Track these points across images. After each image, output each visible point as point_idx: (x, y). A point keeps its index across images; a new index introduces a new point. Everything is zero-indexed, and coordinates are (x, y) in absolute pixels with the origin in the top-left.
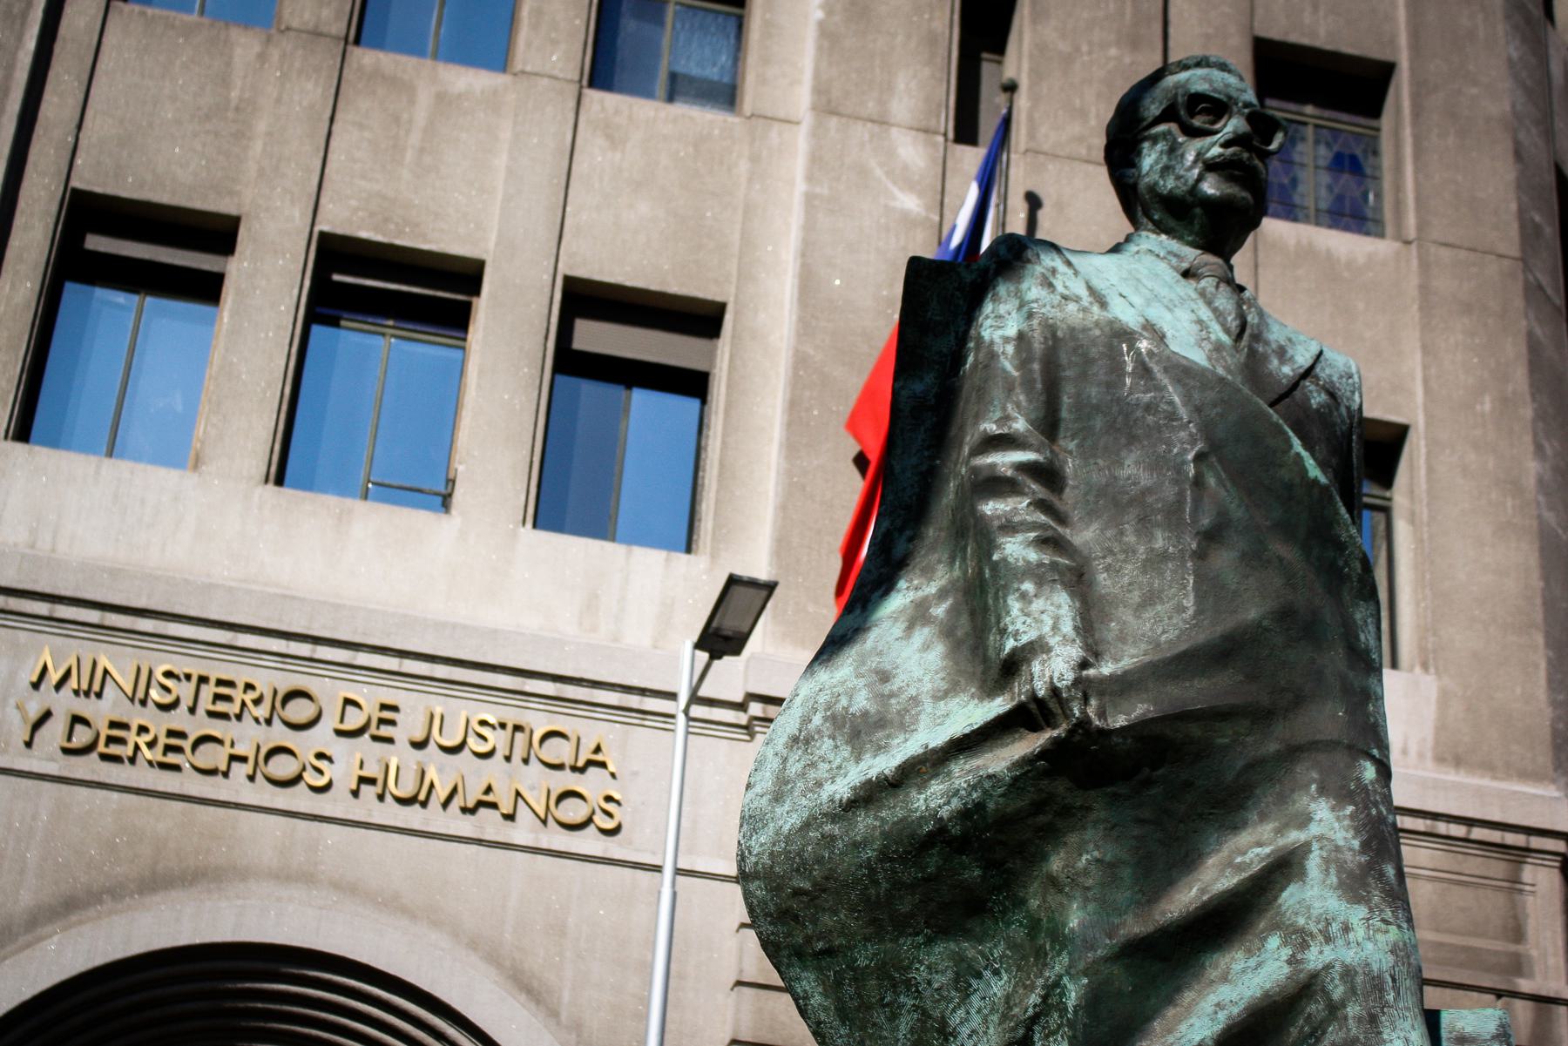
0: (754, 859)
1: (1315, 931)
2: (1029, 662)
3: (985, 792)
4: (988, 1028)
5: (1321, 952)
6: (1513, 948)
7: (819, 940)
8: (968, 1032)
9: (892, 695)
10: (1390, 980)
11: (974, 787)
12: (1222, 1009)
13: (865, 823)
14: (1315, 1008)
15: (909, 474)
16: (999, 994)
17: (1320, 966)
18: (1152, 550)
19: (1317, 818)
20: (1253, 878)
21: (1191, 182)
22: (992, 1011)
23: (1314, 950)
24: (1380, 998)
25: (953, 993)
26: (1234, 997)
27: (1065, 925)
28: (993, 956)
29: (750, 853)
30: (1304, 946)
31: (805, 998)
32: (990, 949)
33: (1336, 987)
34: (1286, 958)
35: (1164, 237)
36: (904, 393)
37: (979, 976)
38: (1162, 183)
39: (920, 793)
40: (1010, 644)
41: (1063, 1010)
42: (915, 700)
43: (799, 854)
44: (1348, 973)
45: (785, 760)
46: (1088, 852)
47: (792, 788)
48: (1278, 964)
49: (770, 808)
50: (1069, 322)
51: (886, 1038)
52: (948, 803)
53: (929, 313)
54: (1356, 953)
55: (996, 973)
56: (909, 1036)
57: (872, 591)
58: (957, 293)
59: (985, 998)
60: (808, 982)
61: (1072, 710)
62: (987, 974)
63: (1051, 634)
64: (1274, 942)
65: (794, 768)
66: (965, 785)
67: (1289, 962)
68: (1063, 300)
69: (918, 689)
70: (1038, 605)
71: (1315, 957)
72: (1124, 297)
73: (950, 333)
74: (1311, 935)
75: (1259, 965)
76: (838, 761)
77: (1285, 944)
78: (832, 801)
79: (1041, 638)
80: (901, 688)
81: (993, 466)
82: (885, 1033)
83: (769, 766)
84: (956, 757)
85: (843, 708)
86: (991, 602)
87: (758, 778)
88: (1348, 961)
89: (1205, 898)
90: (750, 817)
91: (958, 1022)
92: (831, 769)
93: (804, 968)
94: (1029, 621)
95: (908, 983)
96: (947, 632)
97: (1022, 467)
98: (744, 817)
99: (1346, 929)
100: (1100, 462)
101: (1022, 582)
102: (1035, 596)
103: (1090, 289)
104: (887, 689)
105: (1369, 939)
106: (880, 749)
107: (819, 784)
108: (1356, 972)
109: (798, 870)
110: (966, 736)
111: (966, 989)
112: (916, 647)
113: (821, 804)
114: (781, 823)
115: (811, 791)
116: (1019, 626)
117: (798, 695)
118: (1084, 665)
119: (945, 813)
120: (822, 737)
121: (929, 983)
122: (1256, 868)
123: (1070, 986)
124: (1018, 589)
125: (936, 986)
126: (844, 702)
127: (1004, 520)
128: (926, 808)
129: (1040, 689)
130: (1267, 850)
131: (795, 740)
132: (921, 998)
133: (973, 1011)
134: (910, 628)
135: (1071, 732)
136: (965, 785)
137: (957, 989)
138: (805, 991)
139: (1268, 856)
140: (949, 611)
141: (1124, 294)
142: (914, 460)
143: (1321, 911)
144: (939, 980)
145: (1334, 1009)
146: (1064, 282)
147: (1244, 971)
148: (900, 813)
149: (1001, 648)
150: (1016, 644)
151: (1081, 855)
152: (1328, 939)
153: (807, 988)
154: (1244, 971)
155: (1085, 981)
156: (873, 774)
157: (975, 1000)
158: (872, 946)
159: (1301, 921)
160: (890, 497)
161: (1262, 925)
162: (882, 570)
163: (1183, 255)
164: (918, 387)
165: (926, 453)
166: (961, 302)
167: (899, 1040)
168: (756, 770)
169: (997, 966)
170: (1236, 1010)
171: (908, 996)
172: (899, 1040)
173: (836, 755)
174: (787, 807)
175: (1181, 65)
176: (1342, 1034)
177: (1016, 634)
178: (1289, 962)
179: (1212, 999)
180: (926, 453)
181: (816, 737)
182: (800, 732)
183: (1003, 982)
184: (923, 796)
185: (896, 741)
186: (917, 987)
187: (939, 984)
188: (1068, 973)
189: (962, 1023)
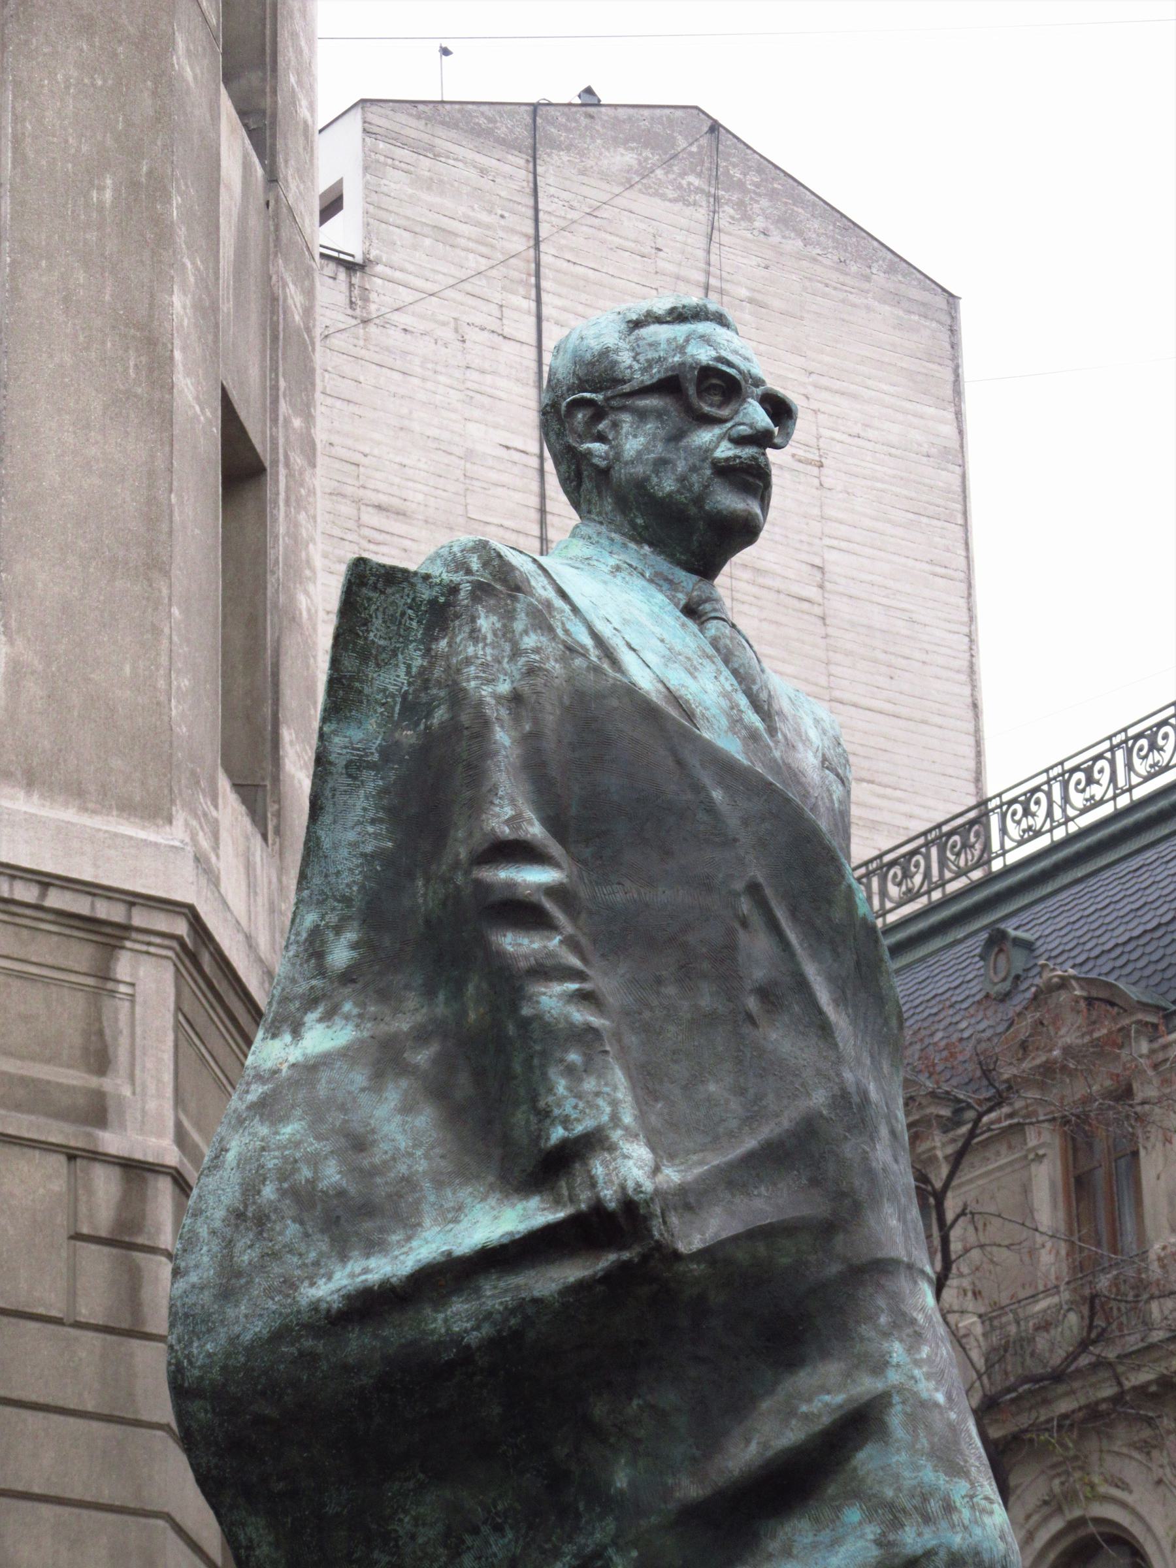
0: (197, 1373)
1: (908, 1506)
5: (920, 1535)
6: (94, 1082)
9: (374, 1171)
11: (512, 1312)
15: (344, 852)
16: (500, 1555)
17: (920, 1552)
19: (894, 1361)
21: (696, 487)
25: (441, 1550)
28: (495, 1508)
29: (190, 1363)
30: (896, 1524)
34: (871, 1537)
35: (646, 549)
36: (336, 740)
37: (475, 1531)
38: (655, 480)
39: (437, 1311)
40: (558, 1134)
42: (409, 1182)
45: (229, 1244)
46: (639, 1396)
47: (248, 1283)
48: (860, 1543)
49: (216, 1307)
50: (577, 684)
52: (477, 1328)
53: (372, 634)
54: (963, 1539)
55: (498, 1529)
58: (410, 612)
59: (480, 1558)
61: (649, 1231)
62: (485, 1529)
63: (611, 1125)
64: (853, 1515)
66: (501, 1308)
67: (879, 1543)
69: (410, 1167)
71: (913, 1539)
72: (634, 650)
73: (397, 665)
74: (904, 1510)
75: (835, 1542)
76: (313, 1255)
77: (869, 1517)
80: (385, 1162)
81: (511, 885)
83: (205, 1248)
85: (307, 1181)
86: (518, 1068)
87: (192, 1263)
88: (955, 1547)
90: (186, 1315)
94: (581, 1105)
97: (552, 891)
98: (176, 1313)
99: (949, 1508)
100: (628, 884)
101: (566, 1051)
102: (585, 1071)
105: (976, 1522)
106: (373, 1246)
107: (290, 1284)
109: (263, 1393)
112: (392, 1104)
114: (237, 1329)
116: (568, 1109)
117: (227, 1151)
118: (656, 1170)
119: (473, 1338)
120: (283, 1218)
121: (413, 1537)
122: (826, 1420)
124: (562, 1061)
125: (420, 1541)
126: (306, 1173)
127: (532, 959)
128: (447, 1330)
129: (611, 1201)
130: (839, 1398)
131: (238, 1216)
135: (645, 1258)
136: (501, 1308)
137: (445, 1546)
138: (251, 1540)
139: (841, 1406)
140: (435, 1061)
142: (351, 836)
143: (914, 1482)
144: (426, 1534)
146: (563, 624)
147: (815, 1546)
148: (409, 1334)
149: (539, 1136)
150: (566, 1134)
151: (631, 1399)
152: (927, 1519)
153: (254, 1536)
155: (635, 1554)
156: (373, 1278)
159: (889, 1493)
160: (317, 880)
161: (831, 1490)
162: (314, 982)
163: (676, 581)
166: (414, 624)
168: (185, 1251)
169: (499, 1521)
173: (309, 1246)
174: (243, 1309)
175: (675, 315)
177: (566, 1122)
178: (879, 1543)
180: (371, 829)
181: (273, 1217)
182: (246, 1206)
183: (506, 1540)
184: (441, 1316)
185: (394, 1238)
186: (396, 1541)
187: (425, 1539)
188: (614, 1543)
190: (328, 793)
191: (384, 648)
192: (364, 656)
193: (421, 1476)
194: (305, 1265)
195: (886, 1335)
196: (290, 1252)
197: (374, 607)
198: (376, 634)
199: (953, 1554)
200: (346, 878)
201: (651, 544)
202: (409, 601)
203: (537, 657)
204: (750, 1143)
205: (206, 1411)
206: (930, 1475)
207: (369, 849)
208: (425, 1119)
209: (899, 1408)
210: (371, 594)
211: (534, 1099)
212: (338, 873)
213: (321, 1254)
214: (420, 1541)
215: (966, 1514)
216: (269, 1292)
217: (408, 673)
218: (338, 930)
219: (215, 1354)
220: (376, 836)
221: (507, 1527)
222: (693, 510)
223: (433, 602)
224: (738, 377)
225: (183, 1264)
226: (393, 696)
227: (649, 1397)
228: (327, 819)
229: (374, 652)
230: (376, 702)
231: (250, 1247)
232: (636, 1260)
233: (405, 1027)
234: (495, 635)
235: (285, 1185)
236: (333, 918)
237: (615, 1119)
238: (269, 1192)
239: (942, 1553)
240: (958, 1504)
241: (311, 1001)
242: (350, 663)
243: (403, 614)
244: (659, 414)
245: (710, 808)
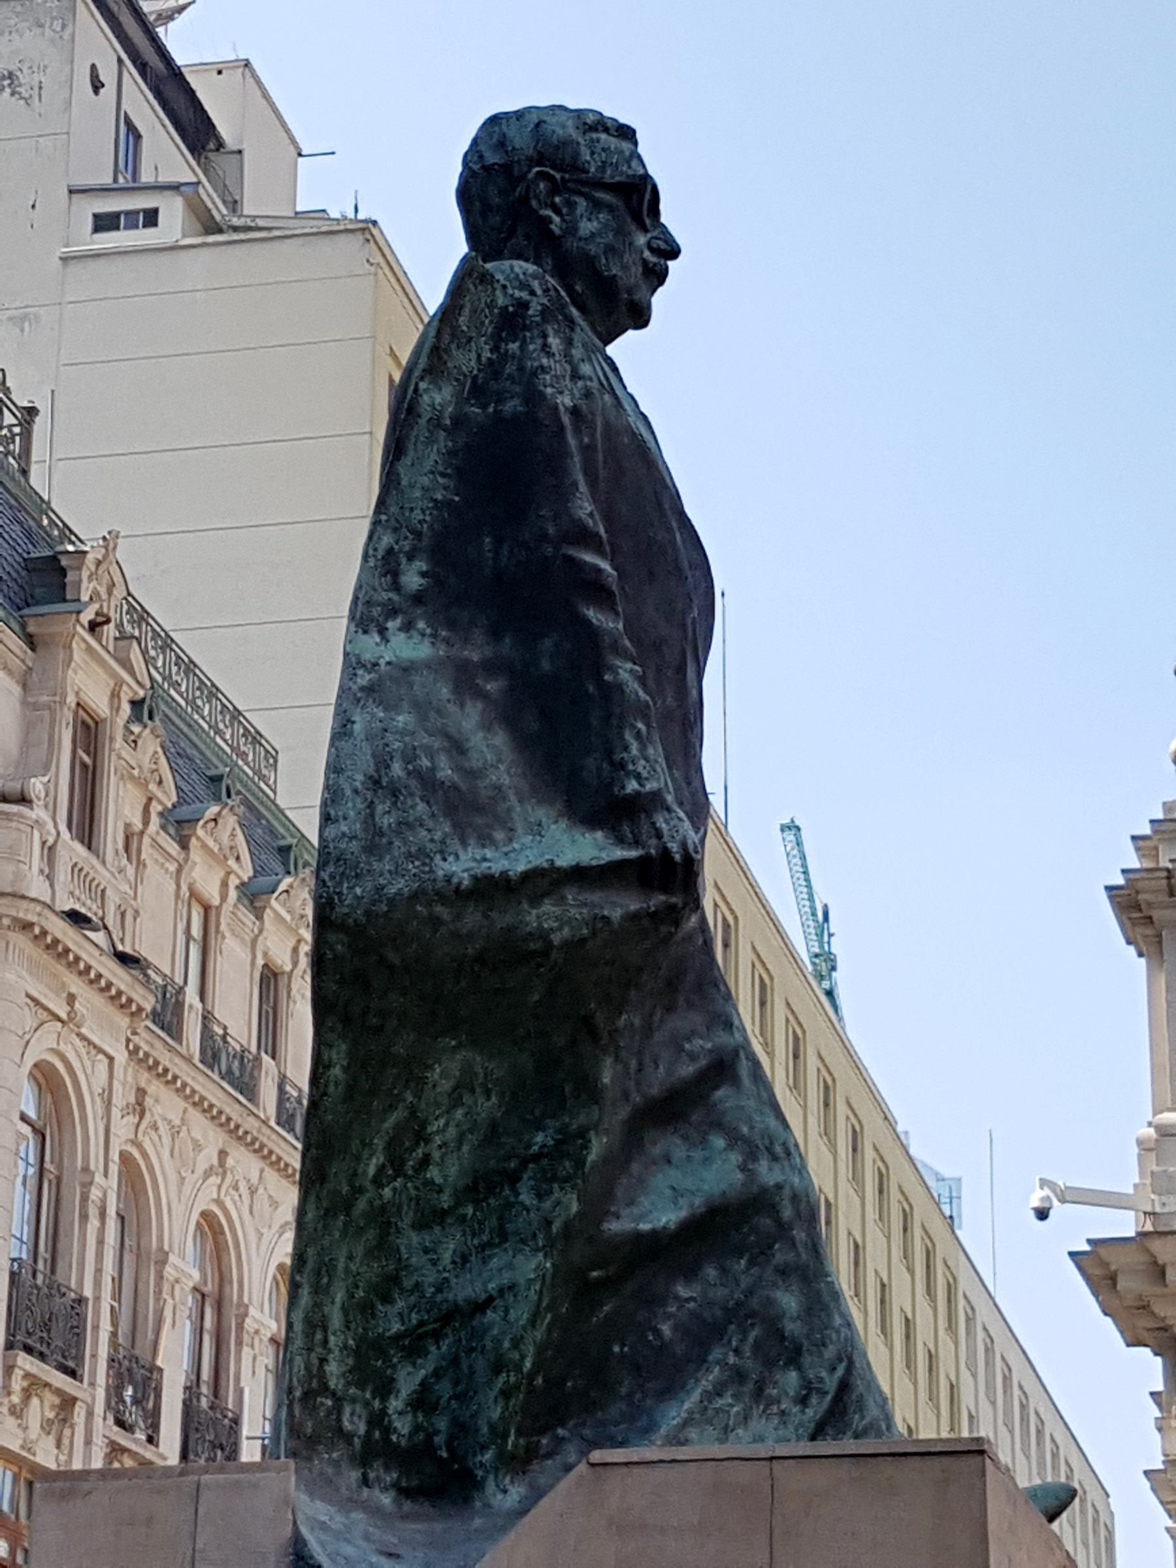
0: (346, 910)
13: (472, 918)
15: (418, 494)
22: (471, 1131)
37: (473, 1091)
39: (534, 908)
40: (632, 786)
41: (580, 1163)
55: (488, 1094)
60: (338, 1054)
95: (422, 1081)
115: (418, 859)
116: (640, 769)
119: (556, 939)
123: (594, 1142)
131: (375, 782)
142: (425, 480)
144: (446, 1086)
148: (508, 919)
151: (621, 1013)
157: (459, 1113)
160: (393, 509)
177: (638, 777)
183: (490, 1103)
184: (534, 912)
189: (438, 1131)
194: (432, 840)
196: (421, 825)
200: (417, 515)
208: (500, 739)
211: (609, 753)
212: (412, 510)
213: (446, 835)
216: (410, 856)
218: (411, 558)
219: (363, 897)
220: (446, 488)
221: (494, 1093)
225: (332, 813)
228: (407, 460)
233: (476, 657)
235: (410, 767)
236: (406, 545)
238: (397, 769)
241: (392, 612)
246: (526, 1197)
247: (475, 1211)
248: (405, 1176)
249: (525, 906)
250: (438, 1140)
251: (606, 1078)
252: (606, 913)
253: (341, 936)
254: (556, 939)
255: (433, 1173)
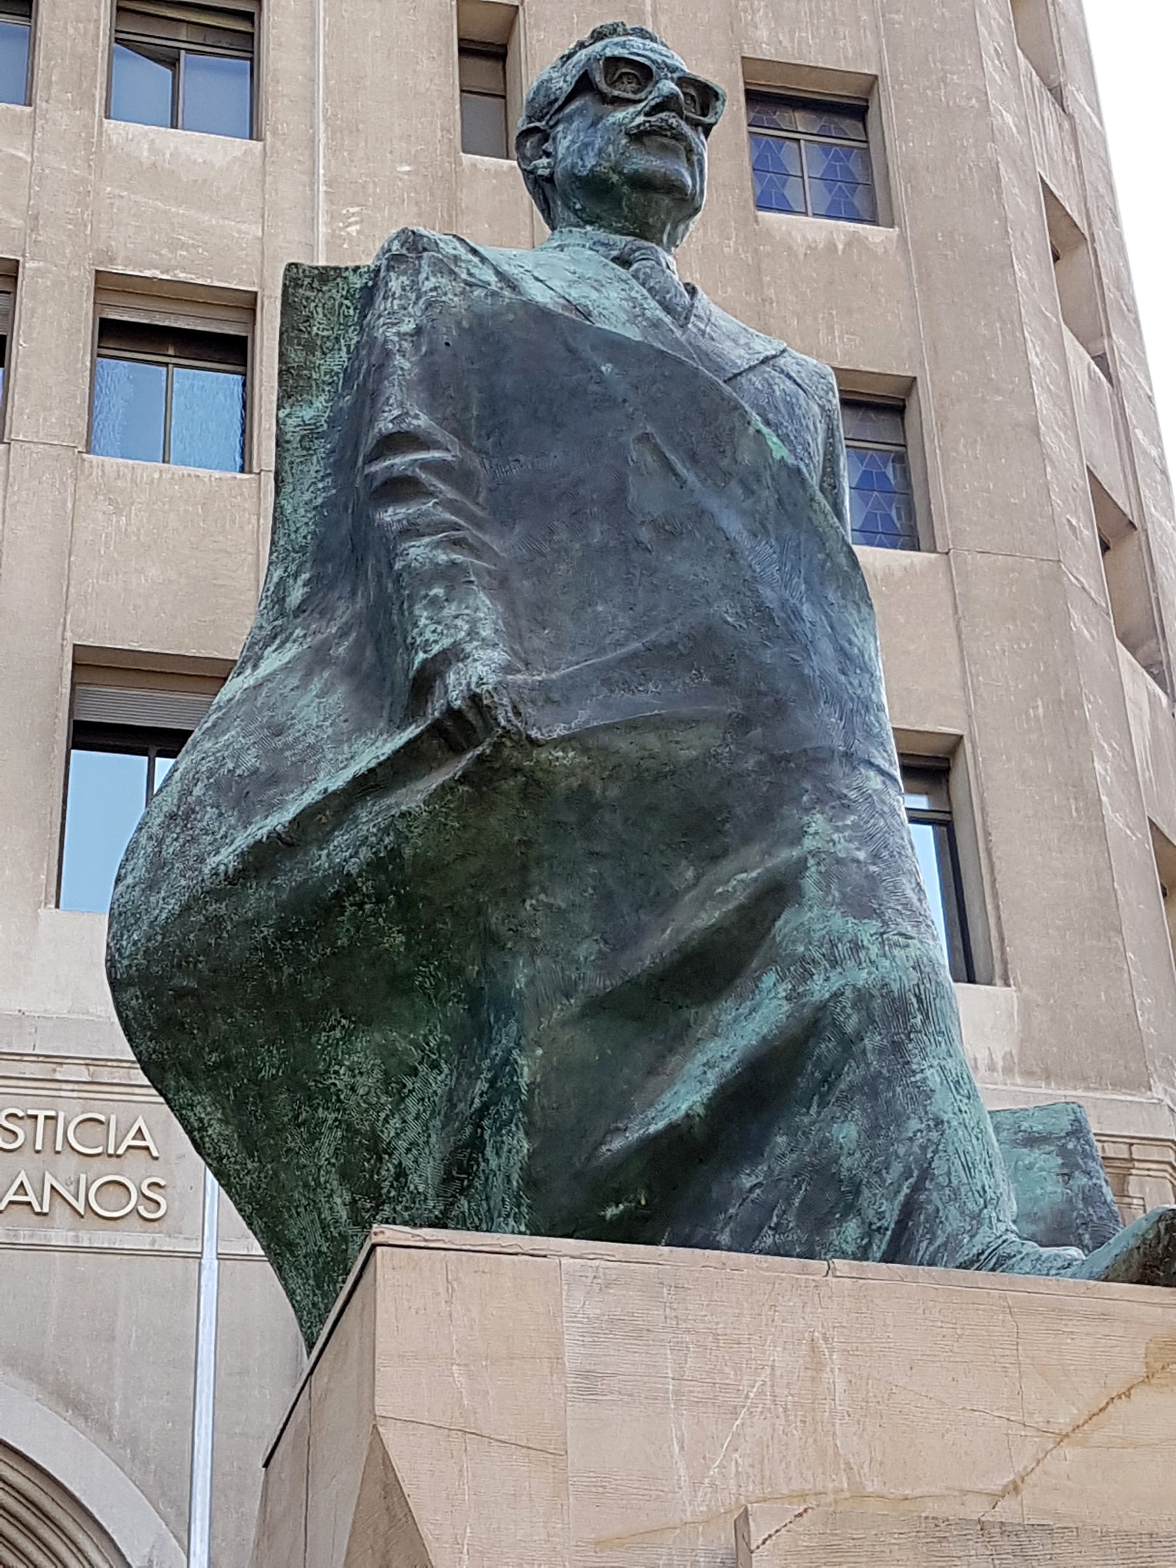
0: (126, 962)
1: (817, 956)
2: (441, 675)
3: (398, 833)
4: (429, 1136)
5: (827, 979)
7: (210, 1053)
8: (406, 1145)
10: (914, 1000)
11: (386, 831)
12: (713, 1067)
13: (256, 897)
14: (826, 1048)
16: (439, 1092)
17: (827, 995)
18: (588, 545)
20: (741, 908)
22: (433, 1116)
23: (818, 979)
24: (905, 1023)
25: (384, 1099)
26: (725, 1051)
27: (510, 987)
28: (428, 1044)
31: (200, 1130)
32: (425, 1036)
33: (849, 1016)
34: (784, 994)
37: (414, 1072)
39: (322, 849)
40: (421, 656)
43: (179, 946)
44: (862, 998)
45: (160, 842)
46: (532, 898)
48: (776, 1002)
50: (475, 310)
51: (305, 1166)
53: (315, 329)
54: (869, 973)
55: (435, 1066)
56: (333, 1161)
57: (266, 646)
58: (347, 302)
59: (423, 1099)
60: (205, 1108)
62: (423, 1069)
64: (769, 979)
65: (169, 850)
66: (375, 830)
67: (788, 998)
68: (468, 288)
70: (450, 610)
71: (819, 988)
72: (541, 281)
73: (340, 349)
75: (754, 1010)
78: (217, 874)
79: (455, 644)
82: (303, 1161)
84: (362, 798)
85: (229, 771)
86: (395, 618)
89: (682, 938)
91: (392, 1134)
92: (216, 840)
93: (197, 1091)
94: (440, 628)
96: (351, 670)
99: (857, 946)
102: (447, 600)
103: (498, 273)
104: (279, 743)
105: (885, 955)
106: (271, 808)
107: (201, 860)
108: (872, 996)
109: (180, 965)
110: (371, 771)
111: (399, 1092)
113: (203, 880)
116: (428, 635)
119: (353, 867)
121: (353, 1089)
122: (741, 897)
124: (427, 596)
125: (361, 1091)
127: (405, 522)
130: (754, 874)
132: (345, 1110)
133: (410, 1118)
134: (308, 676)
135: (498, 746)
136: (375, 830)
138: (201, 1120)
141: (541, 278)
142: (307, 496)
143: (824, 932)
144: (365, 1084)
145: (849, 1044)
147: (736, 1020)
148: (299, 877)
150: (425, 656)
151: (524, 901)
152: (834, 964)
153: (203, 1115)
154: (736, 1020)
155: (540, 1052)
157: (412, 1105)
158: (278, 1049)
164: (308, 414)
165: (320, 485)
166: (351, 312)
167: (321, 1167)
169: (434, 1057)
170: (728, 1066)
171: (328, 1108)
172: (321, 1167)
174: (163, 894)
176: (861, 1072)
178: (788, 998)
179: (701, 1058)
180: (320, 485)
181: (197, 809)
183: (443, 1076)
186: (338, 1096)
187: (367, 1089)
189: (398, 1135)
190: (287, 467)
191: (328, 337)
192: (309, 348)
193: (344, 1021)
195: (807, 810)
197: (313, 304)
198: (319, 327)
199: (859, 990)
200: (304, 531)
201: (591, 223)
202: (344, 293)
203: (434, 294)
204: (635, 645)
205: (137, 998)
206: (840, 922)
207: (319, 501)
209: (813, 869)
210: (308, 293)
213: (230, 827)
214: (361, 1091)
215: (874, 950)
217: (348, 352)
222: (615, 178)
223: (365, 287)
224: (648, 63)
226: (337, 374)
227: (542, 897)
228: (288, 489)
229: (319, 343)
230: (324, 382)
231: (176, 840)
232: (488, 751)
234: (404, 290)
236: (293, 568)
237: (472, 634)
239: (848, 992)
240: (865, 943)
242: (296, 356)
243: (341, 305)
244: (580, 111)
245: (601, 380)
246: (494, 1163)
247: (469, 1202)
248: (390, 1200)
249: (314, 850)
250: (402, 1144)
251: (520, 982)
252: (404, 808)
253: (132, 990)
254: (353, 867)
255: (415, 1182)
